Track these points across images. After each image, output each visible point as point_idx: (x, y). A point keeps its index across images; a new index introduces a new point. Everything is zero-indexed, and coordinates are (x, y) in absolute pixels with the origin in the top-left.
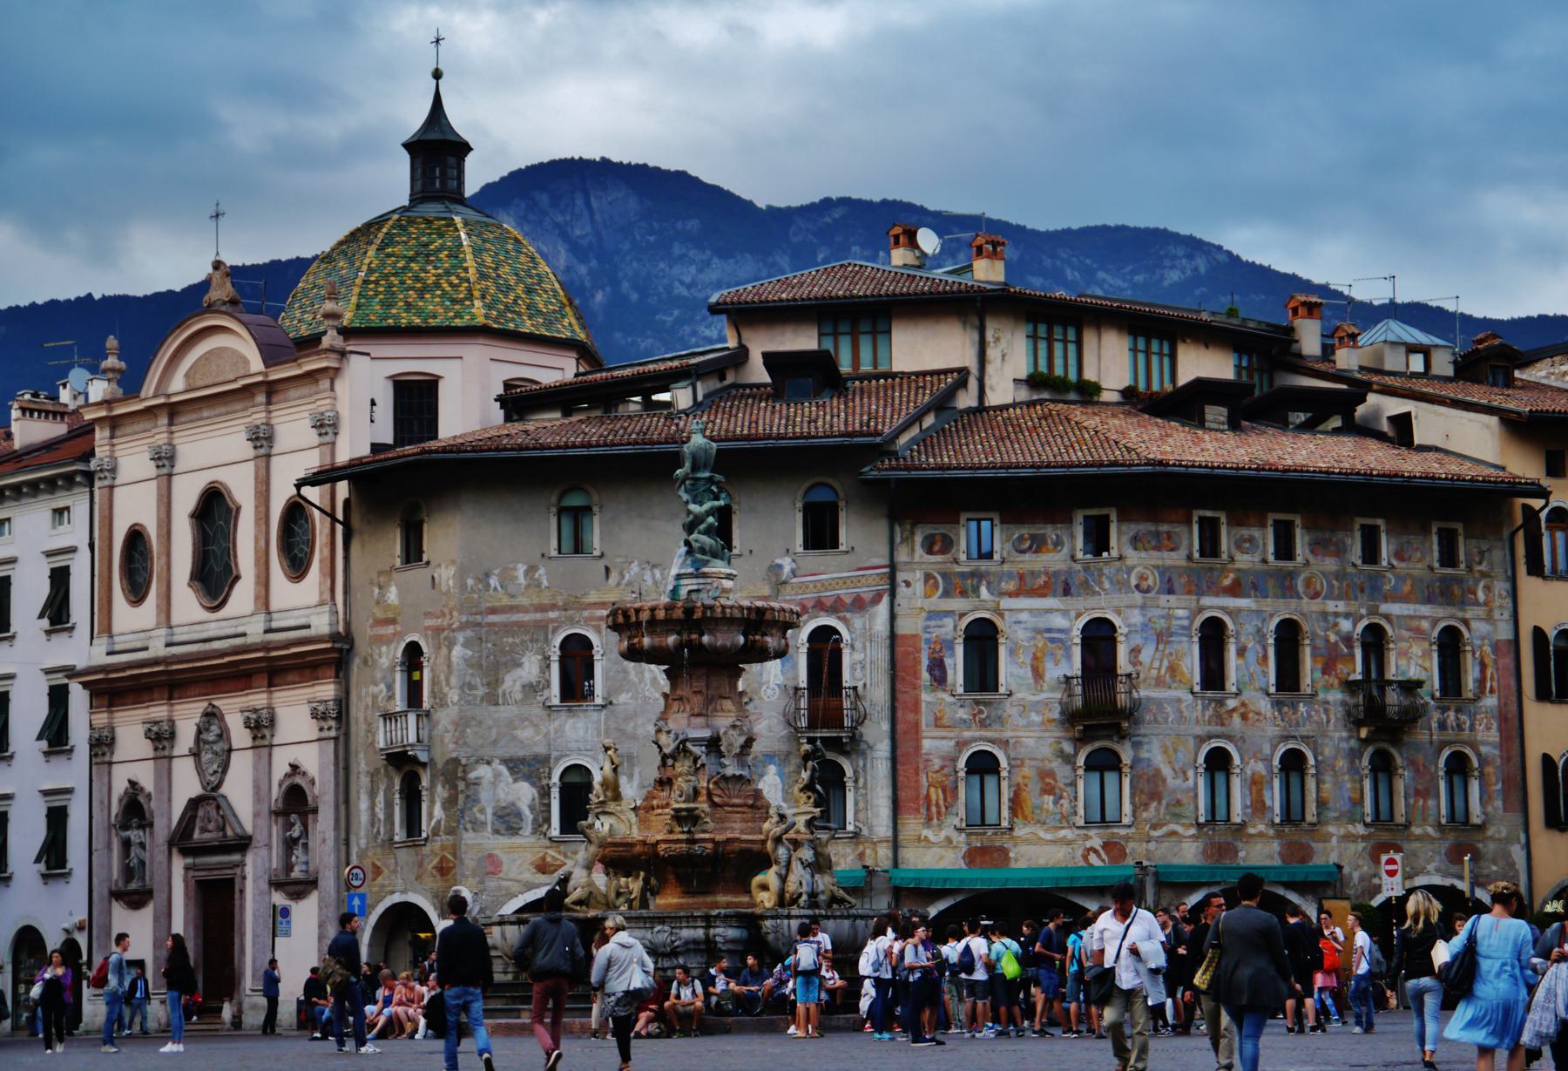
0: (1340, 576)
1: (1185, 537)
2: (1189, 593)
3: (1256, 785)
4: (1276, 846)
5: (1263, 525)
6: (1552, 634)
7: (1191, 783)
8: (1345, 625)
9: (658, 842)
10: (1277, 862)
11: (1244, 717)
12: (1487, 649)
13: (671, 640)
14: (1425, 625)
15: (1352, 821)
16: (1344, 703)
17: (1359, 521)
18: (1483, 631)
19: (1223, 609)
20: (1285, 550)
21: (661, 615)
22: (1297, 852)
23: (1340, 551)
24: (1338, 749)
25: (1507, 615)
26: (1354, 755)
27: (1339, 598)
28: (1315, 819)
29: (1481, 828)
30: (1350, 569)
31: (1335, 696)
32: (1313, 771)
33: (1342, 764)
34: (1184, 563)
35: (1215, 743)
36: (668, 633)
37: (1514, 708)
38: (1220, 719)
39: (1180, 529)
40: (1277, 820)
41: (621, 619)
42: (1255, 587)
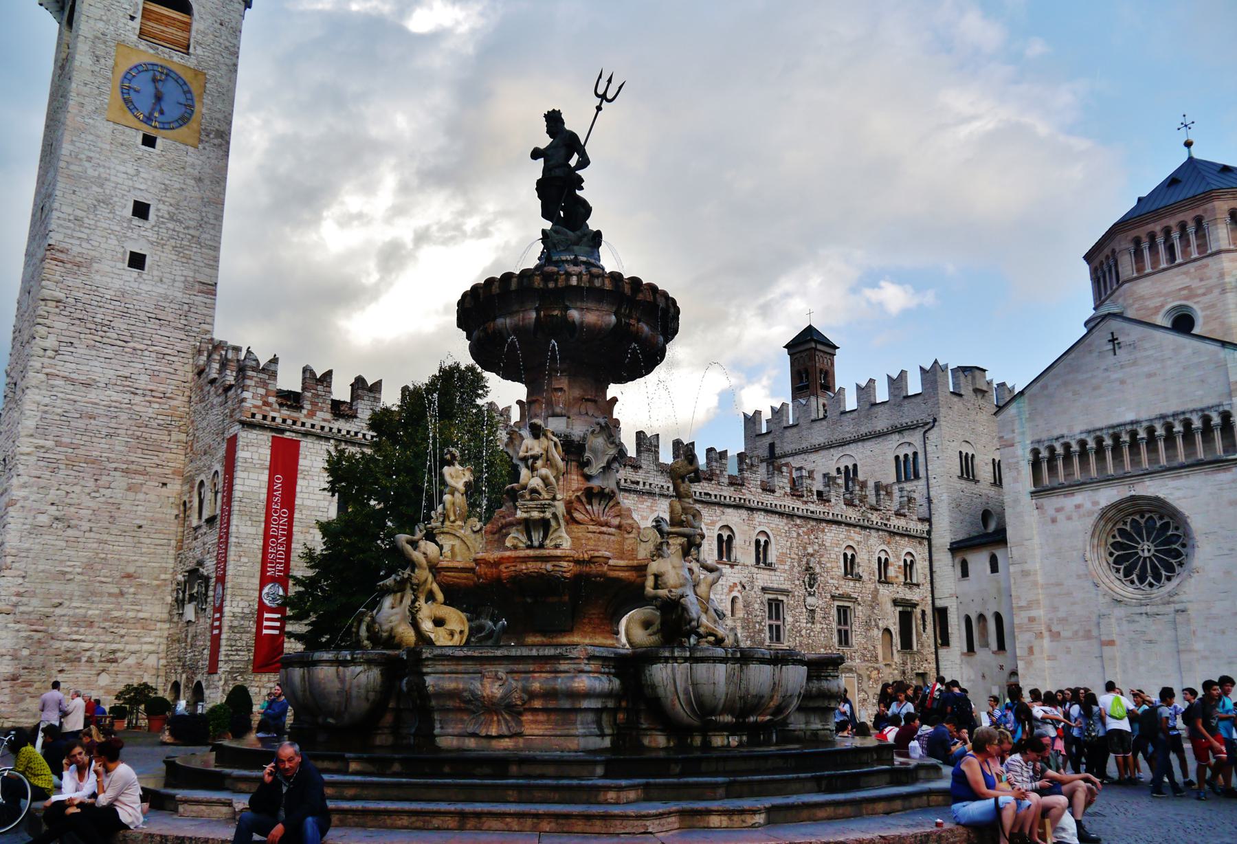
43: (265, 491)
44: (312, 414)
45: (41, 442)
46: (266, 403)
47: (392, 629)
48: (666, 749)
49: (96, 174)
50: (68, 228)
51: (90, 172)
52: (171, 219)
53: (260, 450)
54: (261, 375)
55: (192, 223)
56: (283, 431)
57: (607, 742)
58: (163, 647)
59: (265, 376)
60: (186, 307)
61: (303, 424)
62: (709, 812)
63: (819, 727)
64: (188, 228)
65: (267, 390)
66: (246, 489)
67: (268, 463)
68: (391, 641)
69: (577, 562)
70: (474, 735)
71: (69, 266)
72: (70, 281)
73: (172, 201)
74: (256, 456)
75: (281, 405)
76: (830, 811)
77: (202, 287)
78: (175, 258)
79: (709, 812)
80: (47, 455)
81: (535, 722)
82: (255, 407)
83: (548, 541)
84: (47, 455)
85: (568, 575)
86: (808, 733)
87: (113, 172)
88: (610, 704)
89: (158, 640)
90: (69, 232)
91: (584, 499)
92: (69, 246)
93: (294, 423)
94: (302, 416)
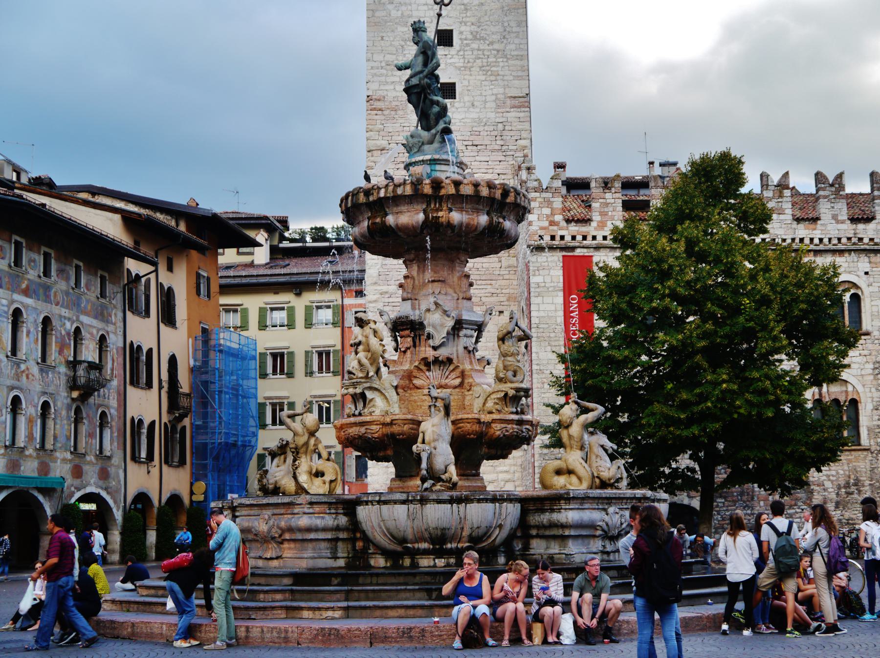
0: (67, 293)
1: (8, 251)
2: (8, 289)
3: (30, 421)
4: (35, 464)
5: (39, 253)
6: (135, 346)
7: (4, 418)
8: (68, 325)
9: (494, 421)
10: (36, 475)
11: (28, 377)
12: (115, 351)
13: (483, 219)
14: (95, 331)
15: (66, 450)
16: (66, 375)
17: (76, 262)
18: (115, 341)
19: (22, 303)
20: (47, 273)
21: (485, 192)
22: (44, 469)
23: (67, 279)
24: (63, 403)
25: (122, 330)
26: (69, 408)
27: (67, 307)
28: (52, 447)
29: (109, 458)
30: (71, 291)
31: (63, 369)
32: (53, 416)
33: (64, 413)
34: (6, 268)
35: (15, 393)
36: (478, 211)
37: (122, 388)
38: (18, 377)
39: (6, 245)
40: (38, 446)
41: (427, 190)
42: (35, 292)
43: (561, 313)
44: (602, 225)
45: (385, 288)
46: (552, 223)
47: (276, 482)
48: (384, 568)
49: (400, 12)
50: (382, 75)
51: (395, 14)
52: (475, 38)
53: (552, 272)
54: (544, 195)
55: (496, 37)
56: (573, 249)
57: (341, 563)
58: (517, 475)
59: (549, 195)
60: (500, 126)
61: (594, 238)
62: (301, 608)
63: (557, 551)
64: (492, 43)
65: (552, 209)
66: (542, 314)
67: (561, 285)
68: (276, 491)
69: (384, 424)
70: (260, 558)
71: (385, 112)
72: (390, 127)
73: (473, 20)
74: (548, 279)
75: (568, 221)
76: (401, 612)
77: (516, 102)
78: (483, 78)
79: (301, 608)
80: (391, 300)
81: (289, 549)
82: (542, 228)
83: (366, 410)
84: (391, 300)
85: (376, 435)
86: (545, 557)
87: (414, 7)
88: (342, 535)
89: (513, 468)
90: (383, 79)
91: (423, 367)
92: (385, 93)
93: (585, 238)
94: (591, 229)
